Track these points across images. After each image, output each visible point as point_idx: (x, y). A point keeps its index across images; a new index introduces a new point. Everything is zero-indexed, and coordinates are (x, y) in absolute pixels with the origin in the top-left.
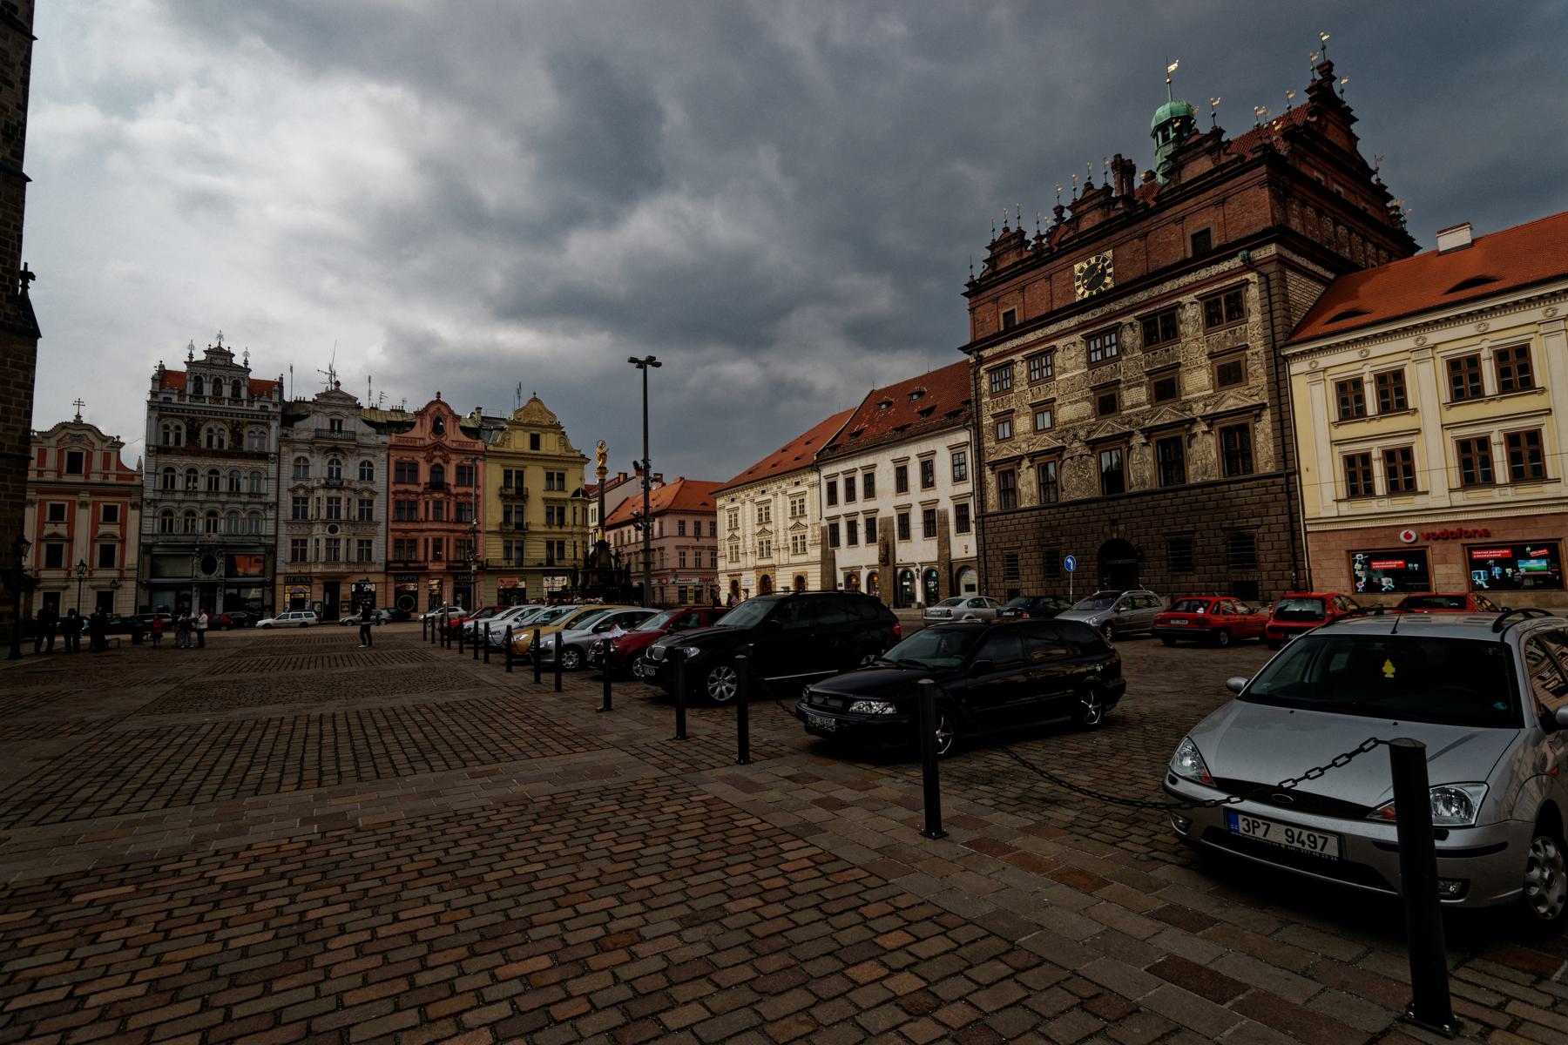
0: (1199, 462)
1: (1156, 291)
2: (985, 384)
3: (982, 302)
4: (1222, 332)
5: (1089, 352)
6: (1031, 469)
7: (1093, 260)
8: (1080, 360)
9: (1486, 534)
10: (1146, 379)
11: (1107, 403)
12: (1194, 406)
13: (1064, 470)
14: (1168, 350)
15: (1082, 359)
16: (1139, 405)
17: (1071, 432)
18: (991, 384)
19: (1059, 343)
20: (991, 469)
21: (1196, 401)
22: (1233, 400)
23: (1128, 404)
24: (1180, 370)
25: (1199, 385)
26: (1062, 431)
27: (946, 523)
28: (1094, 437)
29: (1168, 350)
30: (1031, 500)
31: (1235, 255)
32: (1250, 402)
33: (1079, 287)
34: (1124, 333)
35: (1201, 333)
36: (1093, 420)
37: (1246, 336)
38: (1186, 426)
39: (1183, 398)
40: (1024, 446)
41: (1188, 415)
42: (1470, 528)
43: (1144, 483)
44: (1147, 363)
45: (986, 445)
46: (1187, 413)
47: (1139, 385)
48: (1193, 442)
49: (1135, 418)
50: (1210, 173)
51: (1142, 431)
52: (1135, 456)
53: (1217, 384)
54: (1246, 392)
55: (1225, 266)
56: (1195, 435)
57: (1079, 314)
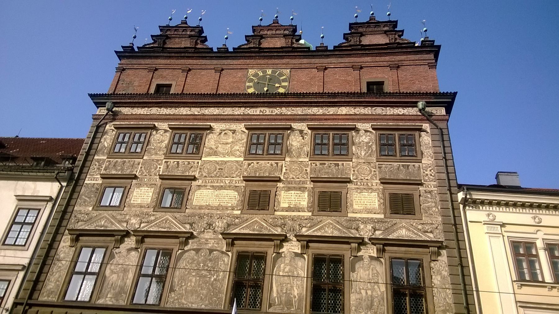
0: (363, 292)
1: (332, 110)
2: (107, 141)
3: (135, 66)
5: (250, 145)
6: (133, 253)
7: (269, 72)
8: (237, 148)
10: (310, 185)
12: (362, 227)
13: (182, 264)
15: (240, 147)
16: (298, 209)
18: (116, 141)
20: (72, 240)
21: (365, 221)
25: (369, 207)
26: (193, 215)
28: (234, 232)
29: (338, 165)
30: (117, 296)
31: (414, 105)
32: (424, 238)
33: (249, 87)
34: (292, 137)
35: (374, 159)
36: (239, 212)
37: (419, 174)
38: (354, 245)
39: (350, 215)
40: (133, 221)
41: (354, 233)
43: (289, 303)
44: (313, 170)
46: (353, 231)
47: (302, 189)
48: (357, 266)
50: (386, 44)
51: (299, 237)
52: (283, 267)
53: (388, 211)
54: (420, 227)
55: (400, 111)
56: (361, 258)
57: (245, 107)
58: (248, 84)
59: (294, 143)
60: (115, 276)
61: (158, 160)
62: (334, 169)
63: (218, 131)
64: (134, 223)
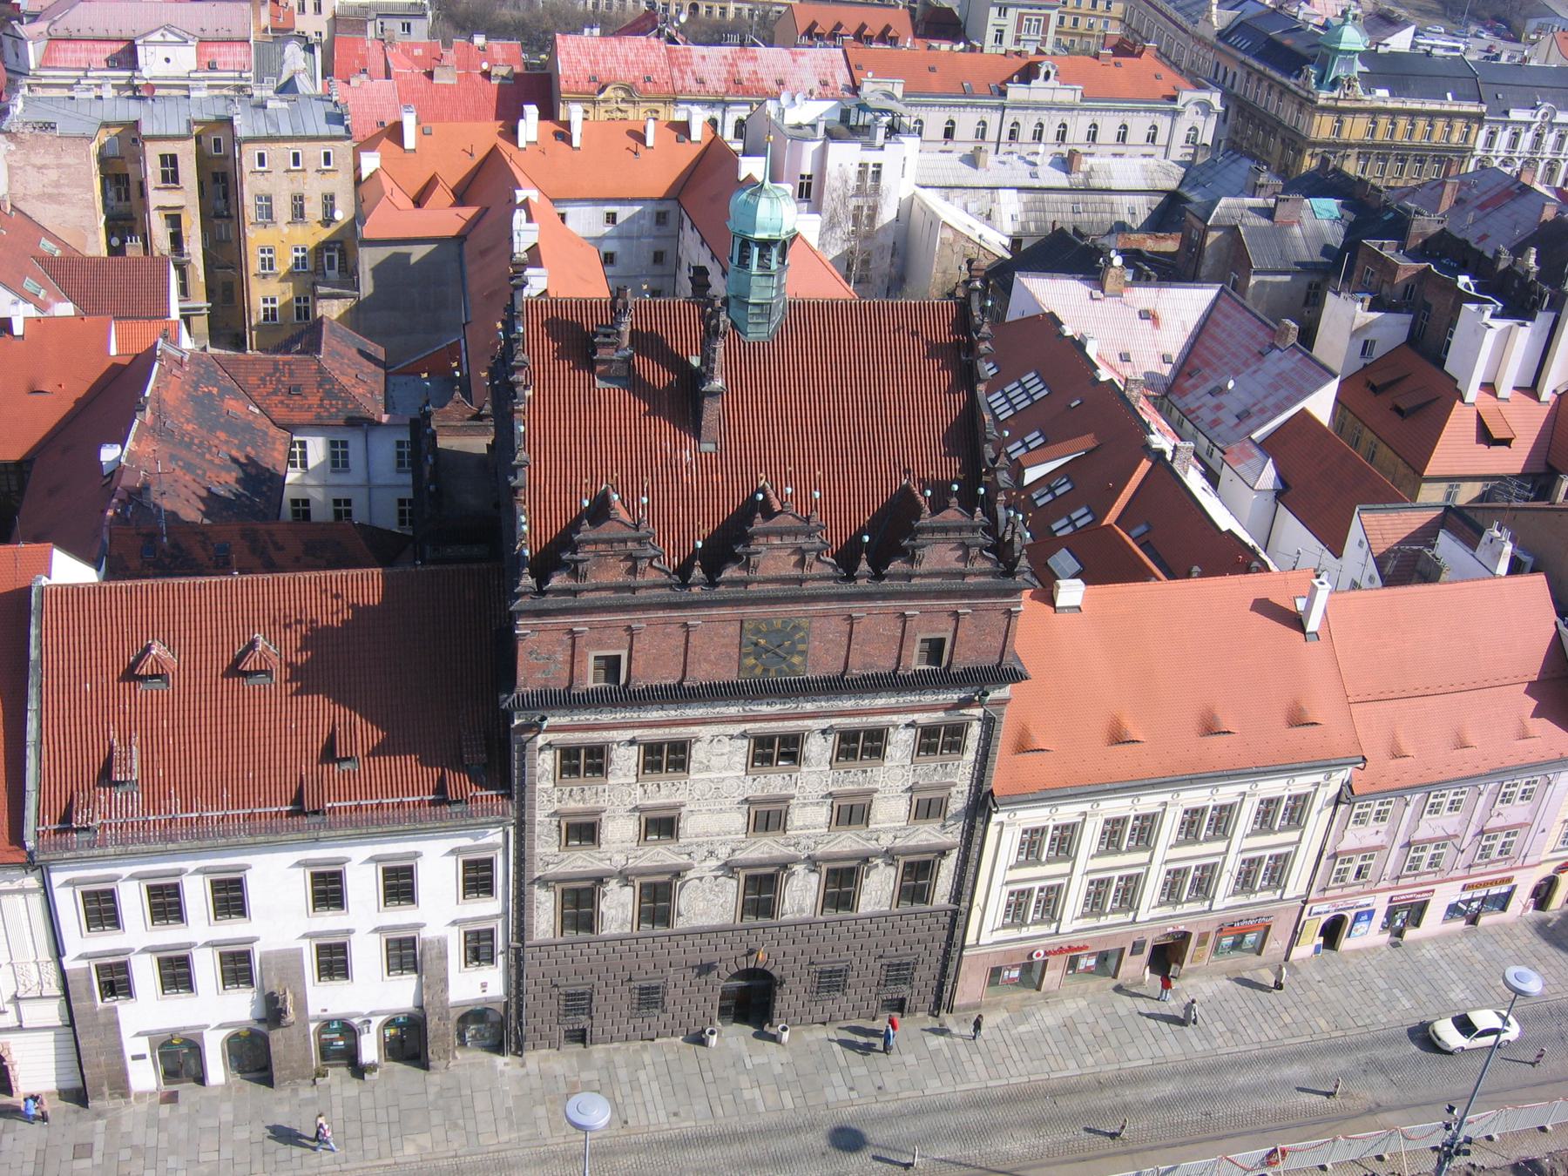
4: (933, 765)
9: (1086, 948)
11: (769, 817)
14: (865, 772)
17: (705, 848)
19: (705, 732)
21: (886, 831)
22: (928, 834)
23: (797, 823)
24: (876, 795)
27: (443, 956)
28: (739, 856)
29: (865, 772)
30: (621, 926)
34: (811, 740)
37: (956, 773)
42: (1081, 945)
43: (801, 910)
45: (537, 851)
46: (874, 842)
49: (804, 842)
58: (744, 650)
59: (813, 749)
60: (613, 912)
61: (629, 784)
62: (861, 777)
63: (709, 737)
64: (619, 861)
